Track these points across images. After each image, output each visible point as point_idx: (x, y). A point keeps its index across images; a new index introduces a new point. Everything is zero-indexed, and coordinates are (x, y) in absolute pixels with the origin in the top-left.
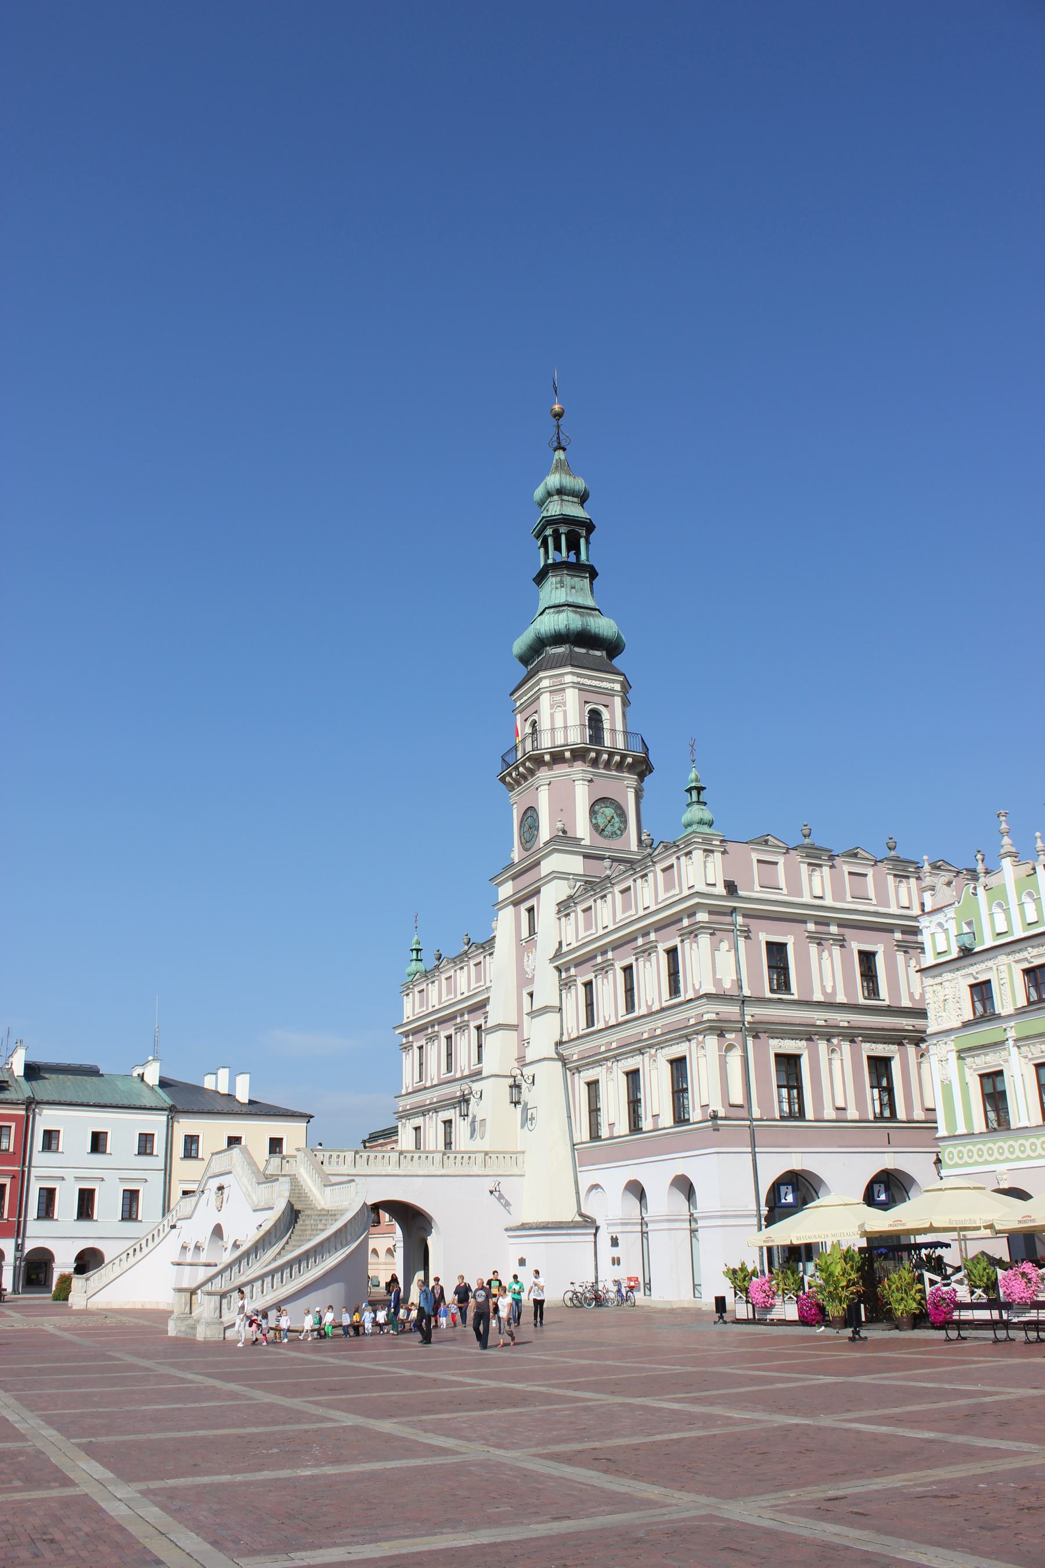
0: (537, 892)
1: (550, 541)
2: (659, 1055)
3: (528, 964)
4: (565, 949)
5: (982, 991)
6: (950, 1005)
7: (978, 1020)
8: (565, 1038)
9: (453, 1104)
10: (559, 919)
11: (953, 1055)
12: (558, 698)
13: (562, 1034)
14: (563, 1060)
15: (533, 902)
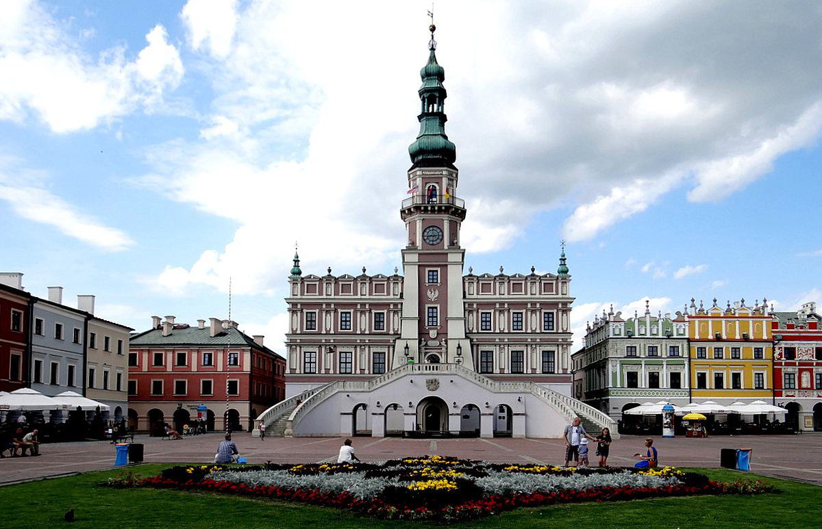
0: (444, 267)
1: (437, 101)
2: (538, 348)
3: (432, 295)
4: (467, 296)
5: (632, 349)
6: (618, 351)
7: (628, 357)
8: (468, 332)
9: (356, 345)
10: (464, 283)
11: (618, 365)
12: (451, 182)
13: (465, 329)
14: (471, 341)
15: (439, 269)
